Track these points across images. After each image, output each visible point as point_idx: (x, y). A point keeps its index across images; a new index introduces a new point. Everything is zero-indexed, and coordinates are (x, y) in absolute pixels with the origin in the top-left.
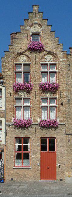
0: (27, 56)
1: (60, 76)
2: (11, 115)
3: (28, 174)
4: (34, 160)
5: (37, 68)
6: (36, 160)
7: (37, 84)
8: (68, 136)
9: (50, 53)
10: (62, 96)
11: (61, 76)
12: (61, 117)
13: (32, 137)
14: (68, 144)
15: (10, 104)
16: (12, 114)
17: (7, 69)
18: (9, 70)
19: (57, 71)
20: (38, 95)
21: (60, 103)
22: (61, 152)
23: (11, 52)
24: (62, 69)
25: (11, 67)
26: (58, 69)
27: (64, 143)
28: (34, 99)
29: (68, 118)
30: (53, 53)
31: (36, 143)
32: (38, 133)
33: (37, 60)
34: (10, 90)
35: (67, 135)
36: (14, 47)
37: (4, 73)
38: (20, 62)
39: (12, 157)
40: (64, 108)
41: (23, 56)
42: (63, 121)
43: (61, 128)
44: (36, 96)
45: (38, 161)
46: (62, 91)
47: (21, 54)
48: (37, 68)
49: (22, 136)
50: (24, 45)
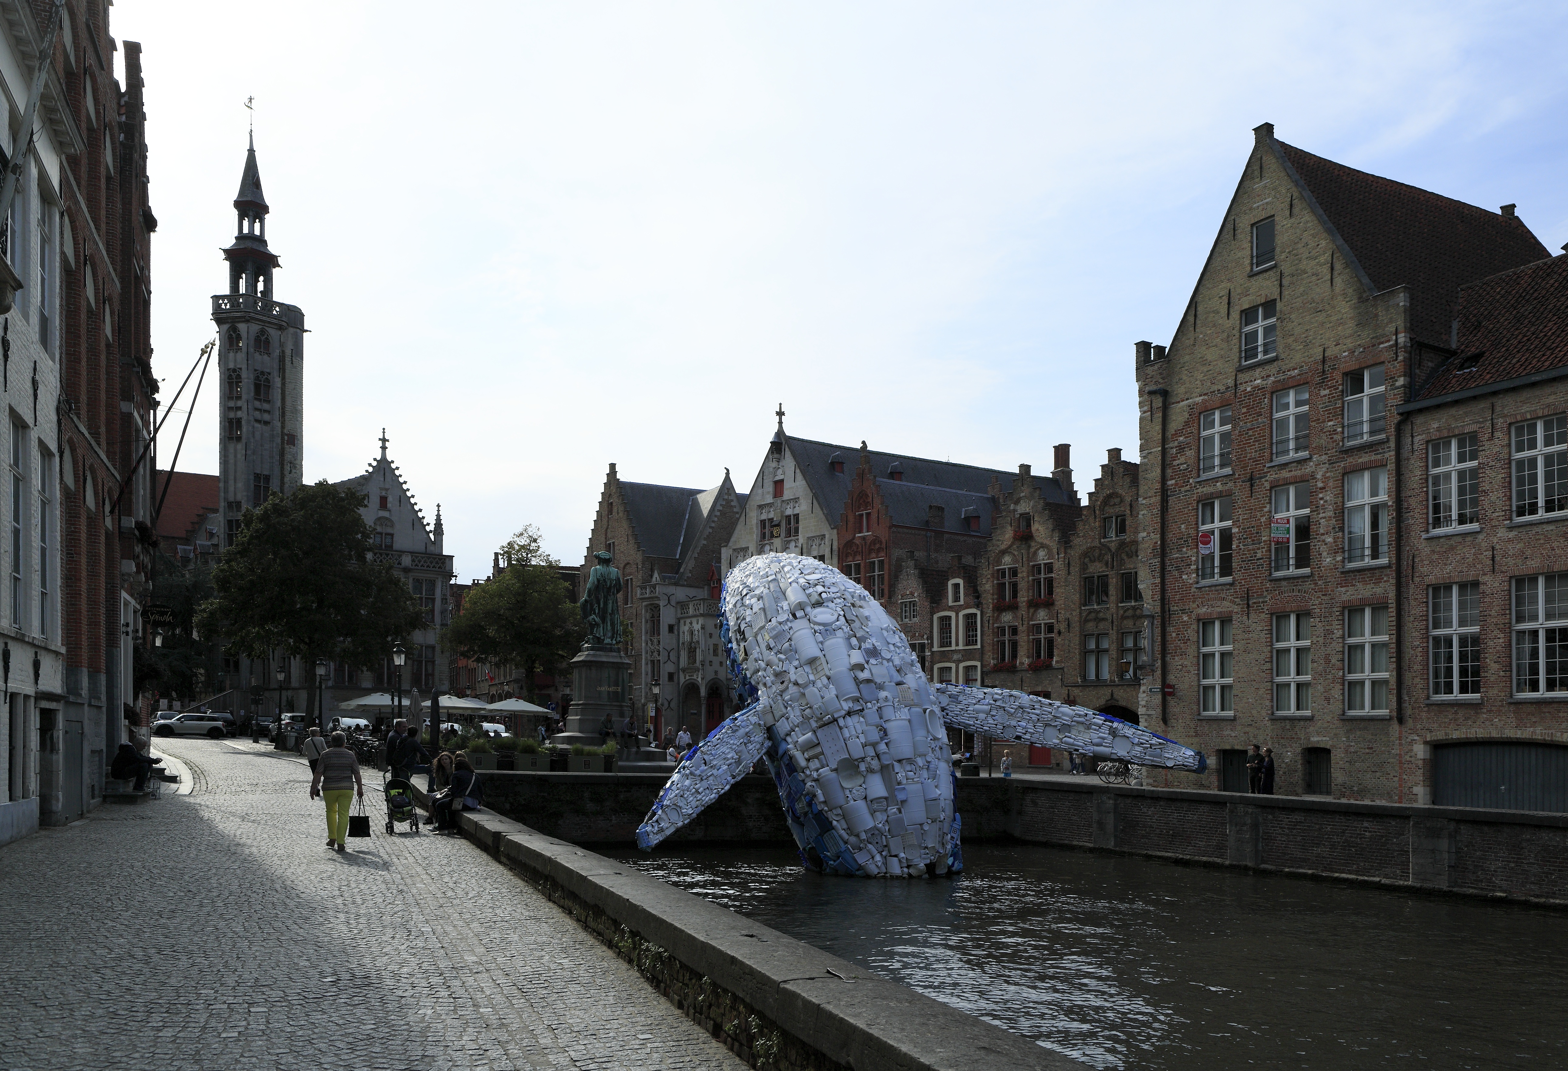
10: (1060, 619)
17: (984, 581)
36: (994, 542)
50: (1007, 536)
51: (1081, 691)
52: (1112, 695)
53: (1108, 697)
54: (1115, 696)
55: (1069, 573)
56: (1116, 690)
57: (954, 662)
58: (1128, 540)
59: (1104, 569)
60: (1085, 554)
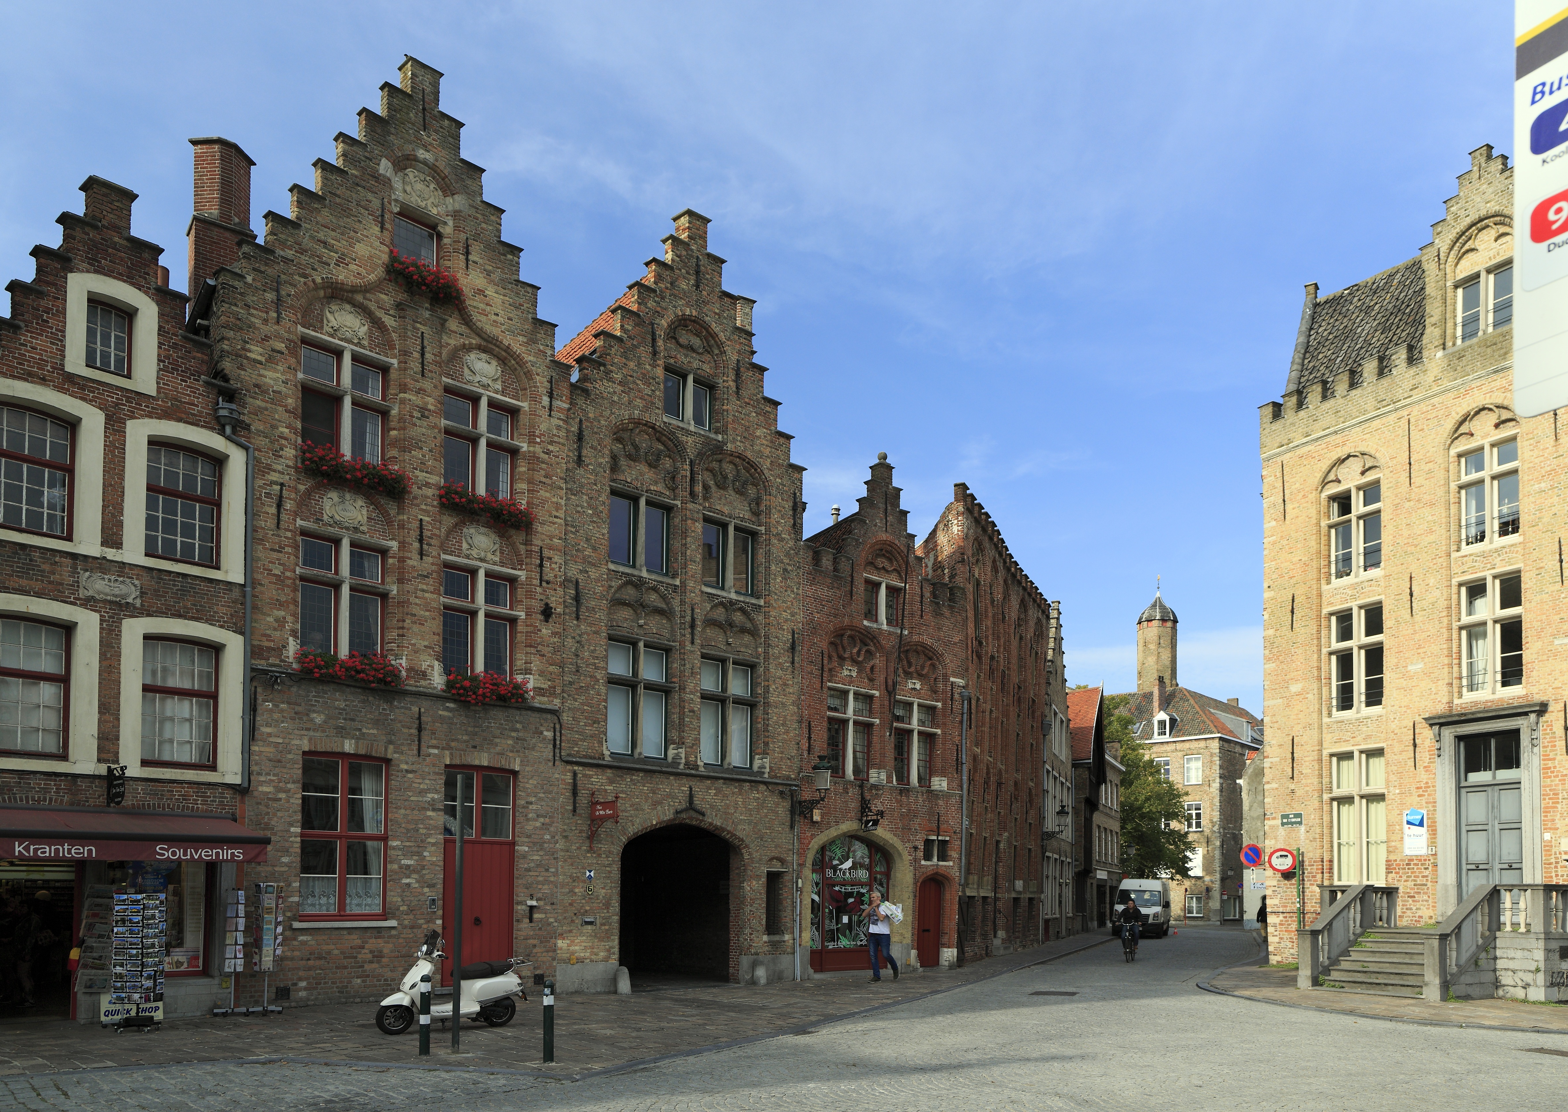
0: (376, 323)
1: (539, 476)
2: (281, 622)
3: (378, 956)
4: (407, 881)
5: (431, 403)
6: (422, 882)
7: (427, 485)
8: (569, 767)
9: (490, 346)
11: (543, 480)
12: (541, 673)
13: (404, 760)
14: (570, 808)
15: (275, 555)
16: (289, 619)
17: (256, 352)
18: (270, 359)
19: (524, 447)
20: (433, 542)
21: (538, 606)
22: (539, 845)
23: (286, 260)
24: (551, 448)
25: (281, 346)
26: (531, 442)
27: (553, 799)
28: (413, 561)
29: (571, 683)
30: (508, 349)
31: (423, 792)
32: (434, 742)
33: (429, 356)
34: (274, 476)
35: (568, 762)
37: (241, 367)
38: (331, 336)
39: (286, 865)
40: (554, 634)
41: (348, 307)
42: (550, 692)
43: (542, 728)
44: (425, 547)
45: (431, 886)
46: (546, 553)
47: (337, 293)
48: (431, 403)
49: (348, 747)
50: (361, 249)
51: (611, 782)
52: (691, 796)
53: (680, 802)
54: (696, 801)
55: (579, 461)
56: (699, 788)
57: (89, 603)
58: (730, 446)
59: (660, 487)
60: (620, 433)
